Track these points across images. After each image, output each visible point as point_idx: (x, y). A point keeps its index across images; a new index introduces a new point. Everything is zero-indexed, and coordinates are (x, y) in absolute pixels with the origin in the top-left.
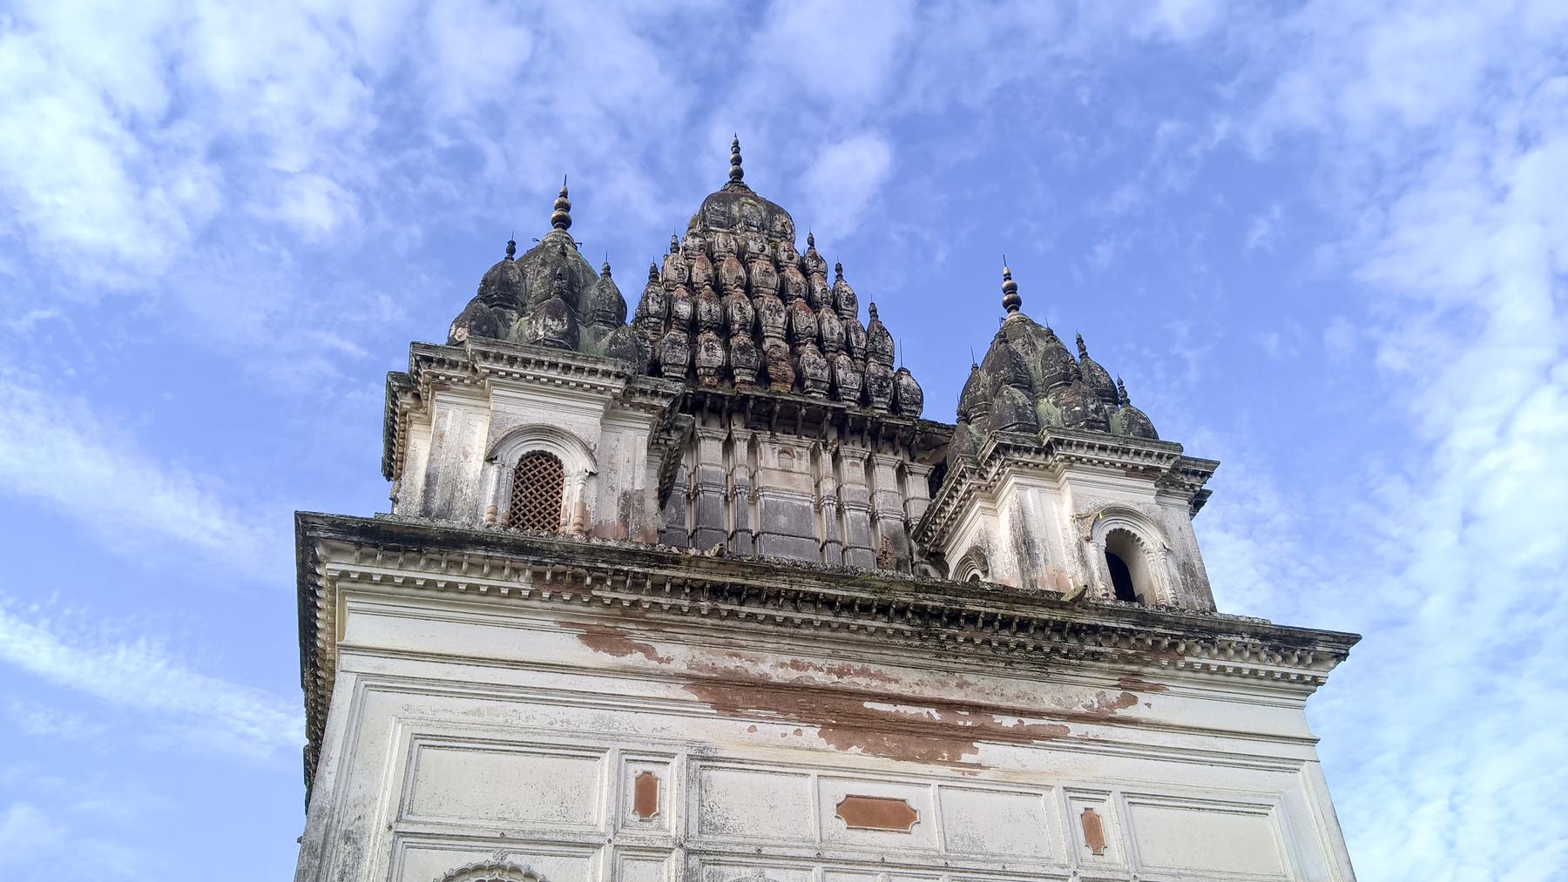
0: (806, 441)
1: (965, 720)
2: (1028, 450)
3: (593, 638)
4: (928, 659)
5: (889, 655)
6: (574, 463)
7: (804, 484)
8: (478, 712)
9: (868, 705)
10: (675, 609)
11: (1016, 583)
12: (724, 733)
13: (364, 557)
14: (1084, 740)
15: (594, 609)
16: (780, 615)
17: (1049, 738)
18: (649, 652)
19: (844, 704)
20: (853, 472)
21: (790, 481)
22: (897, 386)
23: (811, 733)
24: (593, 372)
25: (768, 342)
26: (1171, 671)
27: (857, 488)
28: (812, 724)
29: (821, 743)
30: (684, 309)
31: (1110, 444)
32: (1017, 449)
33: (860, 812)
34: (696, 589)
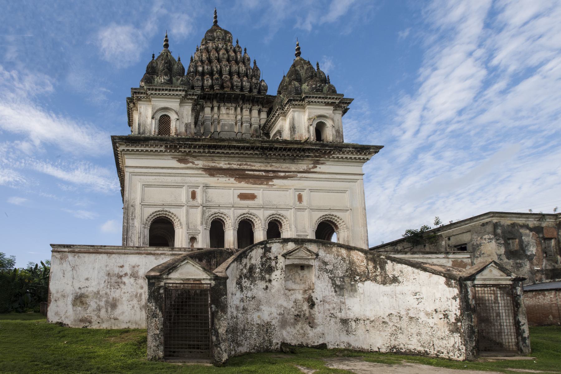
1: (271, 174)
2: (297, 100)
3: (180, 161)
4: (263, 160)
5: (253, 160)
6: (173, 116)
7: (232, 117)
8: (155, 179)
9: (247, 172)
10: (199, 152)
11: (289, 139)
12: (211, 181)
13: (127, 145)
15: (180, 154)
16: (225, 152)
17: (292, 177)
18: (193, 163)
19: (241, 173)
20: (246, 113)
21: (229, 117)
22: (260, 85)
23: (232, 180)
24: (177, 90)
25: (224, 76)
26: (328, 159)
27: (247, 117)
28: (232, 177)
29: (235, 182)
30: (200, 69)
31: (322, 96)
32: (294, 100)
33: (243, 197)
34: (204, 147)
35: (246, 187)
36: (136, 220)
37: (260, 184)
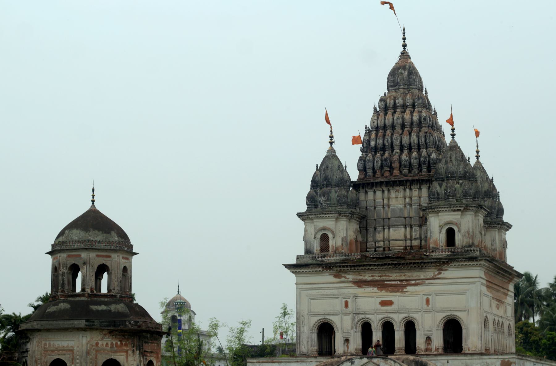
0: (402, 187)
1: (405, 283)
3: (336, 276)
4: (398, 271)
14: (428, 283)
16: (367, 268)
18: (345, 277)
23: (375, 289)
33: (383, 303)
35: (386, 295)
36: (305, 327)
37: (396, 292)
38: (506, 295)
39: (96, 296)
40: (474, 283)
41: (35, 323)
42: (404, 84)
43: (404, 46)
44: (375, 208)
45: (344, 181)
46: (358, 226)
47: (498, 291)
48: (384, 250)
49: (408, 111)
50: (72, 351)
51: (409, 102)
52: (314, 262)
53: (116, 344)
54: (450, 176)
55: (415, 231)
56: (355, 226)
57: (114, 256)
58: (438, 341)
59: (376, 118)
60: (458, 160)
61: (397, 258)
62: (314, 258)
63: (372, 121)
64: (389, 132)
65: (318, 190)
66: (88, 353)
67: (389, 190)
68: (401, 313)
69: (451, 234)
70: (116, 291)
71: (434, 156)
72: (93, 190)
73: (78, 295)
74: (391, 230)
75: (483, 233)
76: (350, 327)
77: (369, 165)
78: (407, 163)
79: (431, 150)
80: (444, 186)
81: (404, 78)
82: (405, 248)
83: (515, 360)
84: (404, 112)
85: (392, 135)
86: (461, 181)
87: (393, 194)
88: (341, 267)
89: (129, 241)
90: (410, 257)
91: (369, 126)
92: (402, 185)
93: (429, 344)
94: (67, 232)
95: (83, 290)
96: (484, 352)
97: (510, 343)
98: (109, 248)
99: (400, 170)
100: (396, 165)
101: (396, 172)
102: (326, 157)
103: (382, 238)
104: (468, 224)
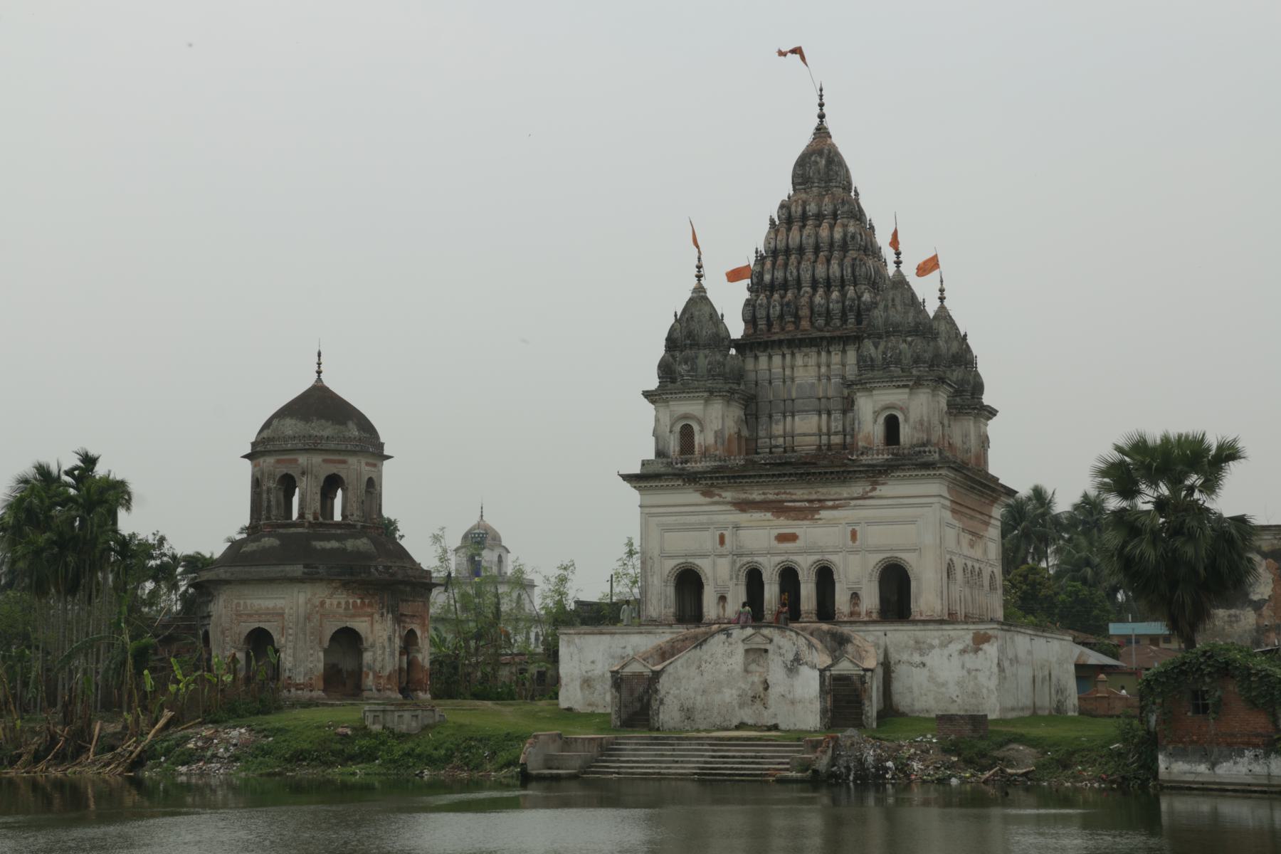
0: (814, 349)
1: (816, 505)
3: (705, 494)
18: (720, 496)
23: (769, 515)
33: (782, 538)
35: (785, 525)
38: (987, 524)
39: (321, 525)
40: (929, 505)
41: (222, 570)
42: (820, 180)
43: (822, 117)
44: (770, 383)
45: (720, 340)
46: (742, 413)
47: (972, 518)
48: (785, 451)
49: (825, 225)
50: (282, 615)
51: (827, 208)
52: (670, 470)
53: (355, 603)
54: (893, 330)
55: (836, 420)
56: (736, 412)
57: (352, 460)
58: (871, 600)
59: (773, 235)
60: (905, 305)
61: (805, 463)
62: (670, 464)
63: (767, 241)
64: (793, 258)
65: (677, 354)
66: (308, 618)
67: (793, 354)
68: (810, 554)
69: (892, 426)
70: (355, 517)
71: (866, 297)
72: (319, 355)
73: (294, 525)
74: (797, 418)
75: (946, 422)
76: (727, 577)
77: (761, 313)
78: (823, 309)
79: (863, 287)
80: (881, 347)
81: (821, 169)
82: (820, 447)
83: (996, 632)
84: (819, 226)
85: (799, 263)
86: (909, 339)
87: (799, 360)
88: (712, 479)
89: (377, 437)
90: (825, 462)
91: (762, 249)
92: (815, 346)
93: (856, 604)
94: (275, 422)
95: (301, 515)
96: (946, 617)
97: (995, 604)
98: (343, 447)
99: (811, 322)
100: (804, 312)
101: (805, 324)
102: (691, 299)
103: (781, 432)
104: (921, 408)
